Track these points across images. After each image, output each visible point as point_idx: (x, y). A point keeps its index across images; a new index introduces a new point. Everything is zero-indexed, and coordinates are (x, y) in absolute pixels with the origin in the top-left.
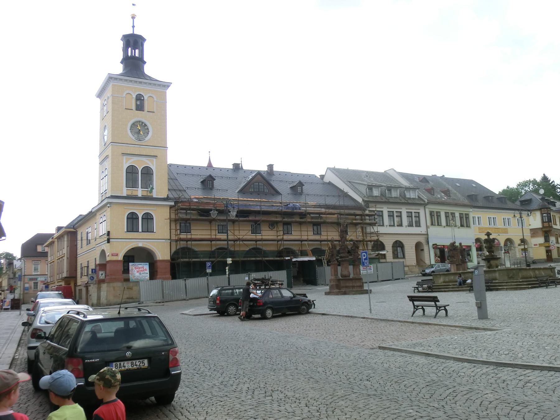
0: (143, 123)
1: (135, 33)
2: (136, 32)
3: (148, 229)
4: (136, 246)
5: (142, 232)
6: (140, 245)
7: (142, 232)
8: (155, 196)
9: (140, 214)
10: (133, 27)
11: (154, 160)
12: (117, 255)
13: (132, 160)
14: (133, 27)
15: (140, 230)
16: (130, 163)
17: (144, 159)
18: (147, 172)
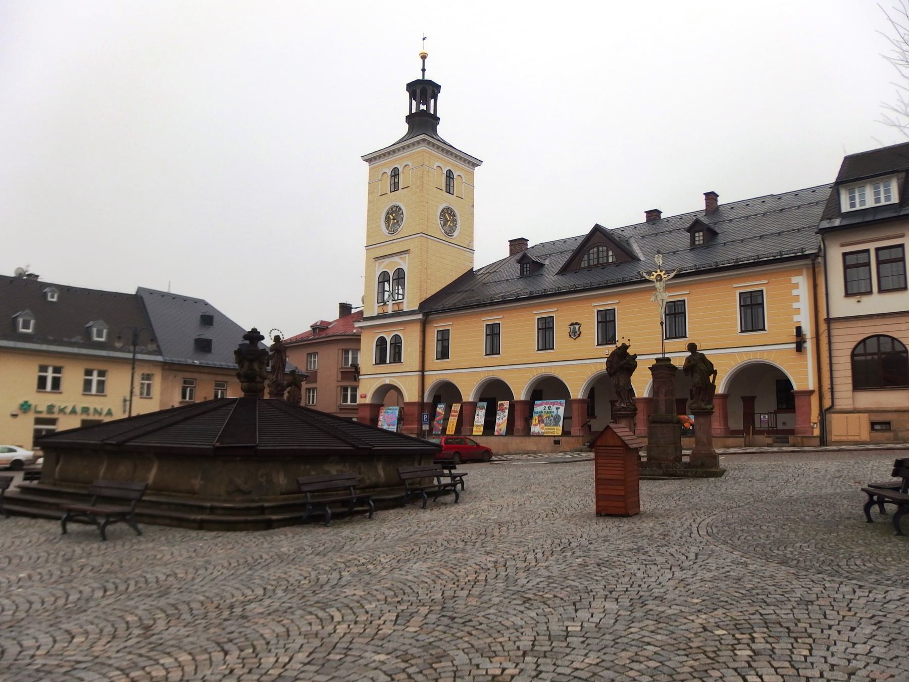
0: (397, 207)
1: (426, 78)
2: (428, 77)
3: (397, 357)
4: (383, 383)
5: (390, 363)
6: (387, 382)
7: (390, 363)
8: (405, 310)
9: (388, 337)
10: (424, 70)
11: (407, 255)
12: (365, 397)
13: (384, 264)
14: (424, 70)
15: (388, 361)
16: (383, 268)
17: (396, 259)
18: (400, 276)
